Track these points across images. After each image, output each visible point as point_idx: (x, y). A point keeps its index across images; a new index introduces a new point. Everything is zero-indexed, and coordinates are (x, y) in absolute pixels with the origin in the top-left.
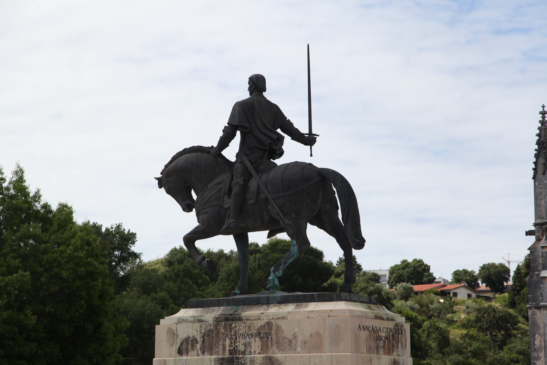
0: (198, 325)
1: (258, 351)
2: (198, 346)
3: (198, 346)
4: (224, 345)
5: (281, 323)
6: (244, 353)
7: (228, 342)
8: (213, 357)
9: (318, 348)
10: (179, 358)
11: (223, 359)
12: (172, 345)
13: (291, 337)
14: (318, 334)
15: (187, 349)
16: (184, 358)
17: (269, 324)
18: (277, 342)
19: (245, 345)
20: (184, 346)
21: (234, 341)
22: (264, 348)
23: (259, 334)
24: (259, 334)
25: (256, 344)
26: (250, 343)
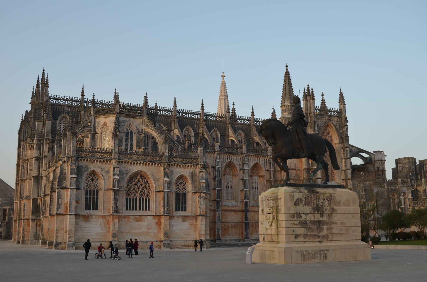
0: (303, 194)
1: (327, 205)
2: (303, 202)
3: (303, 202)
4: (314, 203)
5: (335, 195)
6: (322, 206)
7: (315, 201)
8: (310, 207)
9: (349, 205)
10: (295, 207)
11: (314, 208)
12: (292, 201)
13: (339, 201)
14: (348, 200)
15: (298, 203)
16: (298, 207)
17: (331, 195)
18: (334, 202)
19: (322, 203)
20: (297, 202)
21: (318, 201)
22: (329, 204)
23: (327, 199)
24: (327, 199)
25: (326, 203)
26: (324, 202)
